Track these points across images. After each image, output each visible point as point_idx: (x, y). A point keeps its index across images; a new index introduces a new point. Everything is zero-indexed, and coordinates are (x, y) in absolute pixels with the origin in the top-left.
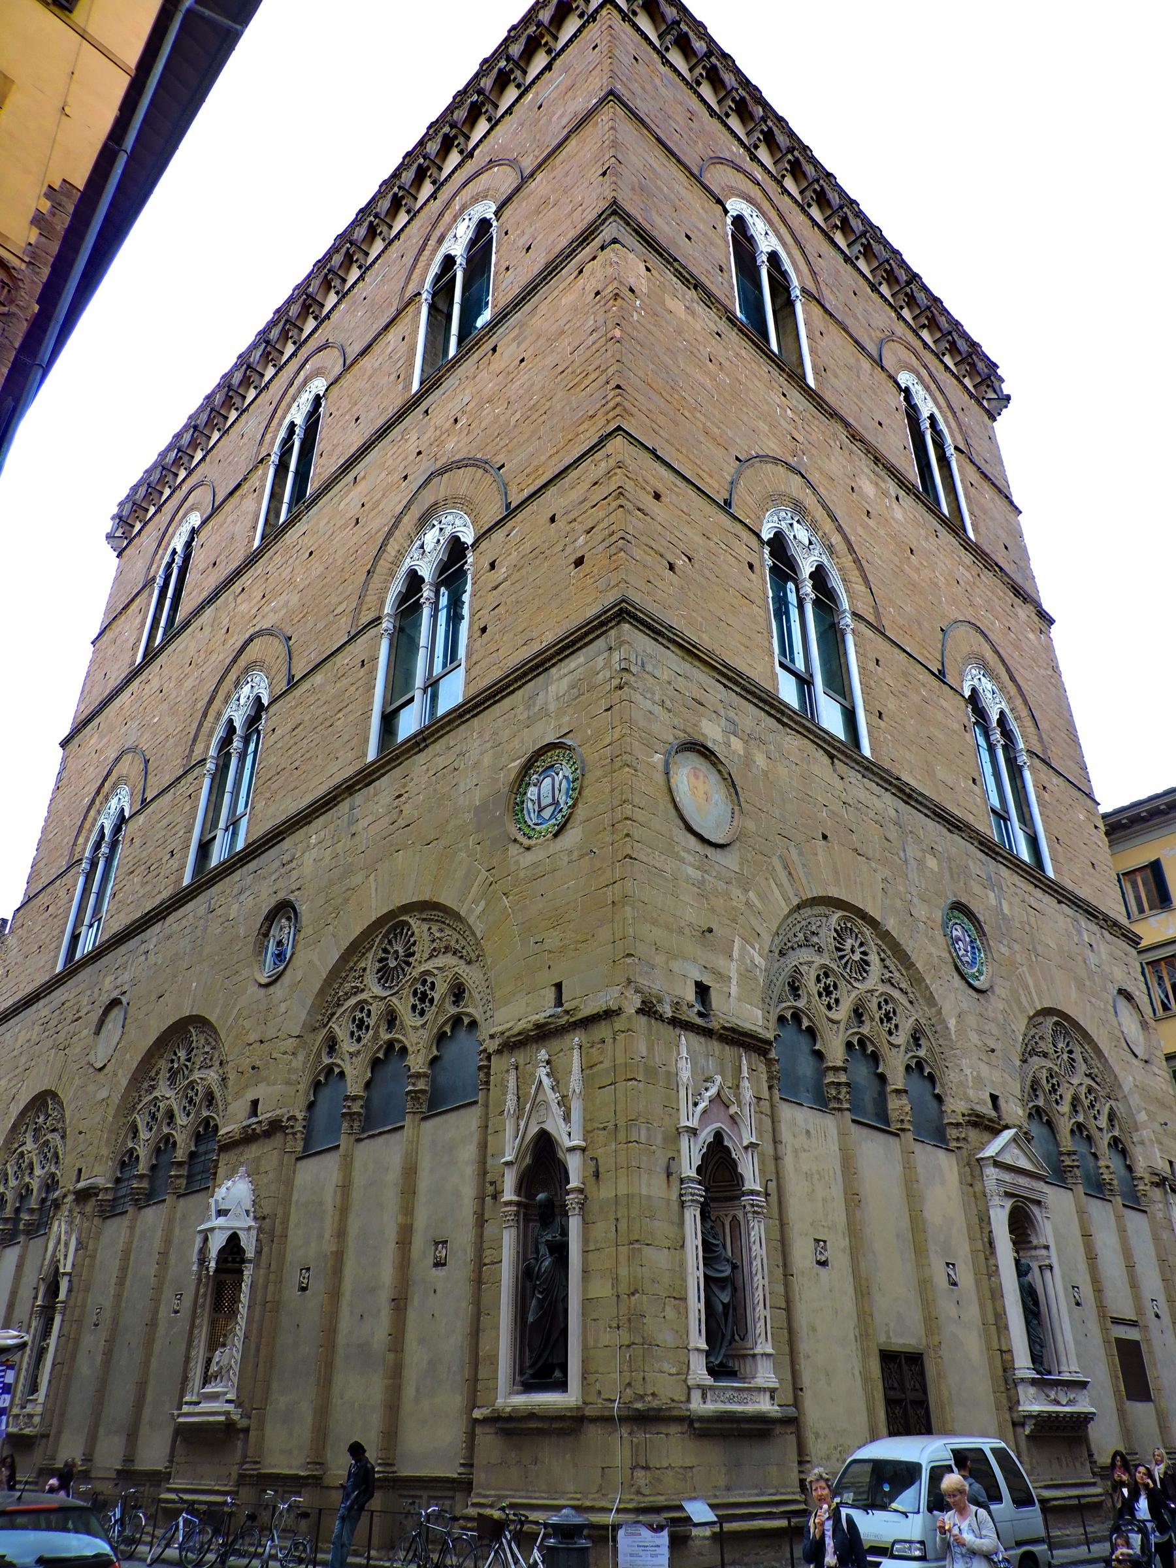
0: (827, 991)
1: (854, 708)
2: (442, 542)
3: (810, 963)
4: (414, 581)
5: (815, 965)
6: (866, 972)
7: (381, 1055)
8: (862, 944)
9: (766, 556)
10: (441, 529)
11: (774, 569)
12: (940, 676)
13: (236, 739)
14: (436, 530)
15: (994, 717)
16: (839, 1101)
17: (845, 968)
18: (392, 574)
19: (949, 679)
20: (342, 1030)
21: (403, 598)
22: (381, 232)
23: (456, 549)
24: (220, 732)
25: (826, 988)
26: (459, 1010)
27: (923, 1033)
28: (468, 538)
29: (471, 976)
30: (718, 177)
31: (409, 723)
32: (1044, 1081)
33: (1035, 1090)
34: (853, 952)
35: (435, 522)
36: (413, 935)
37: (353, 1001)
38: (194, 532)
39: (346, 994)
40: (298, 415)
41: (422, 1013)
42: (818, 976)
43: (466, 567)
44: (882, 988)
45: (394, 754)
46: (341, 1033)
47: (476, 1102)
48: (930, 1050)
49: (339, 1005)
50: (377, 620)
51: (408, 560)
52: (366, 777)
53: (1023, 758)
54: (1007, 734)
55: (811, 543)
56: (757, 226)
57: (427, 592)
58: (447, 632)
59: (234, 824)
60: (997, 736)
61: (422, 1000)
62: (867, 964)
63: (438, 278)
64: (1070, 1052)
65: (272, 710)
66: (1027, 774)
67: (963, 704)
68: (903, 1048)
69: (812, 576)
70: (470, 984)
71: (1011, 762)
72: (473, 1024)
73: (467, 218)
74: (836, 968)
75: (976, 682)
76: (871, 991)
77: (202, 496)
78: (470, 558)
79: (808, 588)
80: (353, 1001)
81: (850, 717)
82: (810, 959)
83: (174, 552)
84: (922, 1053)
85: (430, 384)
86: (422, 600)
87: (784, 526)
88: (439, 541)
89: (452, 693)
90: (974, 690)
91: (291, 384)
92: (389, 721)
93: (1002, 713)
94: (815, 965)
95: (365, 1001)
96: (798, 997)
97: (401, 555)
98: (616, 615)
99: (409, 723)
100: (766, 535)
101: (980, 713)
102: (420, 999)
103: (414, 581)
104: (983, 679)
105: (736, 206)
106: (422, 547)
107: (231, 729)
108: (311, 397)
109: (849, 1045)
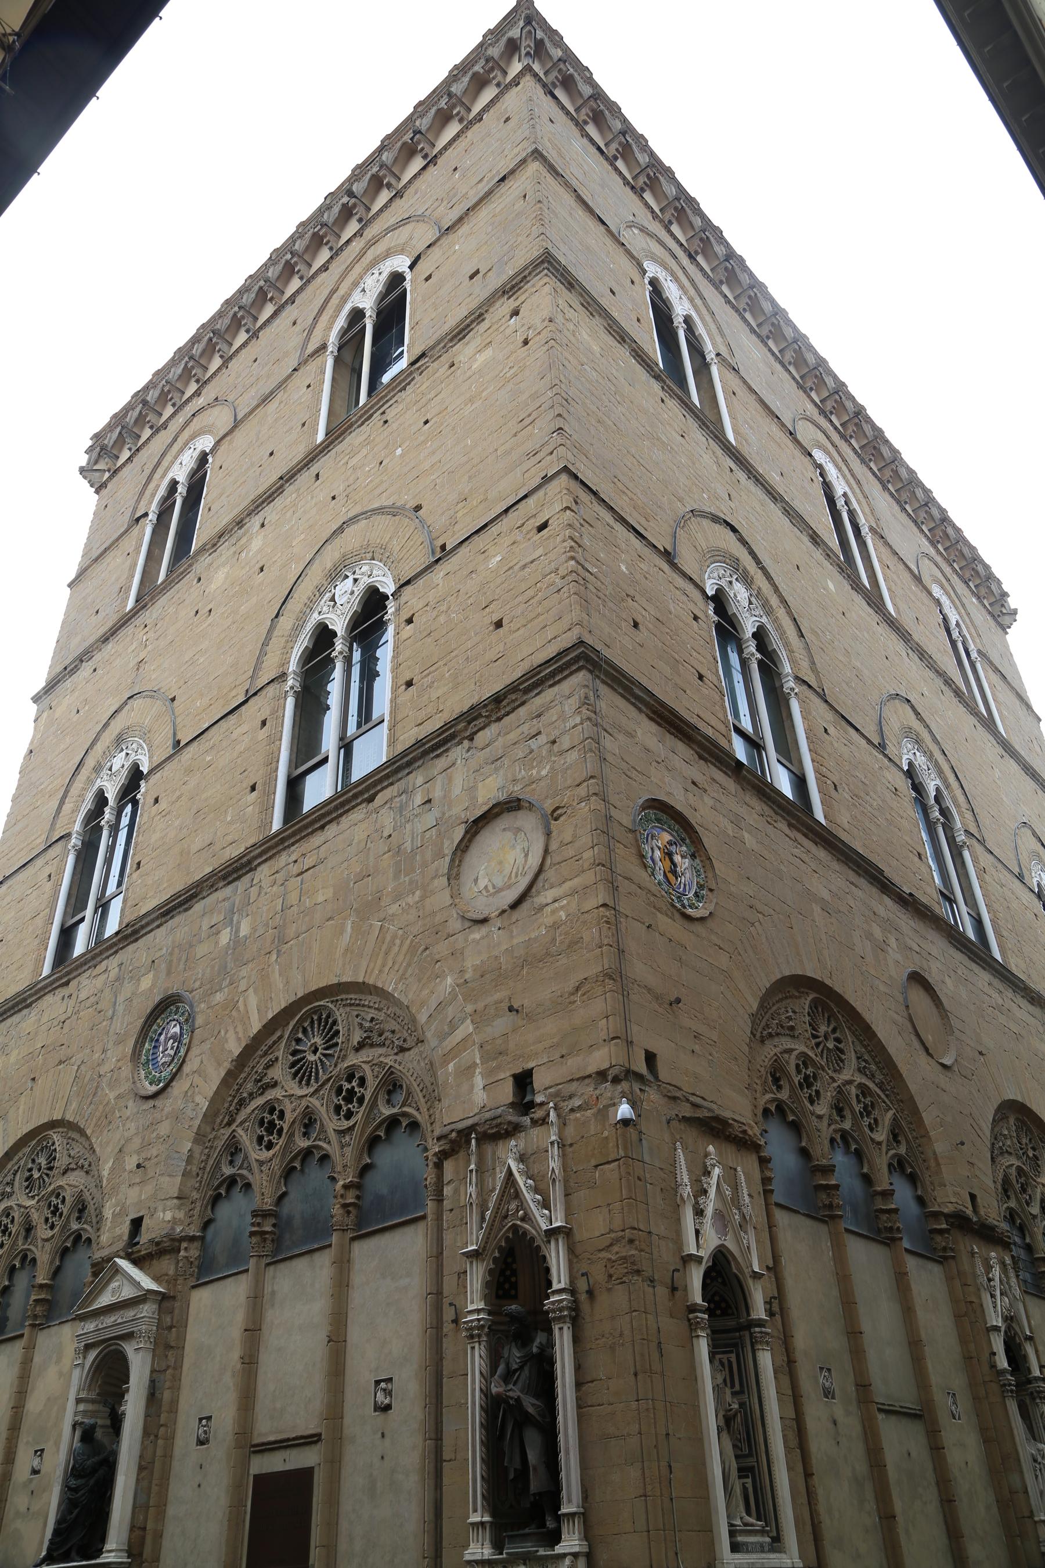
0: (808, 1082)
1: (804, 775)
3: (789, 1051)
4: (324, 636)
5: (795, 1053)
6: (842, 1061)
8: (834, 1031)
9: (711, 612)
10: (356, 580)
11: (719, 627)
12: (881, 747)
13: (107, 810)
14: (350, 580)
15: (933, 793)
16: (830, 1206)
17: (822, 1056)
18: (297, 629)
19: (891, 750)
21: (309, 655)
22: (299, 271)
24: (87, 805)
25: (806, 1078)
26: (395, 1110)
27: (900, 1127)
28: (388, 587)
29: (409, 1066)
30: (635, 240)
31: (319, 788)
32: (1014, 1182)
33: (1005, 1191)
34: (826, 1038)
35: (349, 574)
36: (335, 1023)
37: (260, 1101)
39: (251, 1094)
40: (181, 472)
41: (349, 1115)
42: (797, 1066)
43: (386, 617)
44: (860, 1079)
45: (300, 824)
46: (246, 1139)
47: (423, 1217)
48: (909, 1148)
49: (242, 1103)
51: (315, 615)
52: (271, 847)
53: (961, 837)
54: (944, 812)
55: (750, 603)
56: (672, 291)
57: (339, 645)
58: (361, 690)
59: (103, 906)
60: (936, 814)
61: (348, 1100)
62: (842, 1051)
63: (344, 332)
64: (1034, 1149)
65: (154, 779)
66: (966, 854)
67: (904, 777)
68: (884, 1146)
69: (755, 635)
70: (410, 1080)
71: (951, 840)
72: (414, 1126)
73: (376, 272)
74: (814, 1057)
75: (912, 757)
76: (850, 1082)
78: (391, 607)
79: (751, 647)
80: (260, 1101)
81: (800, 782)
82: (789, 1046)
84: (902, 1150)
85: (336, 433)
86: (333, 654)
87: (723, 583)
88: (352, 593)
89: (371, 754)
90: (911, 764)
91: (175, 440)
92: (295, 786)
93: (938, 790)
94: (795, 1053)
96: (779, 1088)
97: (310, 605)
98: (577, 659)
99: (319, 788)
100: (710, 592)
101: (918, 788)
102: (344, 1099)
103: (324, 636)
104: (918, 754)
105: (652, 269)
106: (333, 599)
107: (101, 800)
108: (196, 454)
109: (832, 1141)
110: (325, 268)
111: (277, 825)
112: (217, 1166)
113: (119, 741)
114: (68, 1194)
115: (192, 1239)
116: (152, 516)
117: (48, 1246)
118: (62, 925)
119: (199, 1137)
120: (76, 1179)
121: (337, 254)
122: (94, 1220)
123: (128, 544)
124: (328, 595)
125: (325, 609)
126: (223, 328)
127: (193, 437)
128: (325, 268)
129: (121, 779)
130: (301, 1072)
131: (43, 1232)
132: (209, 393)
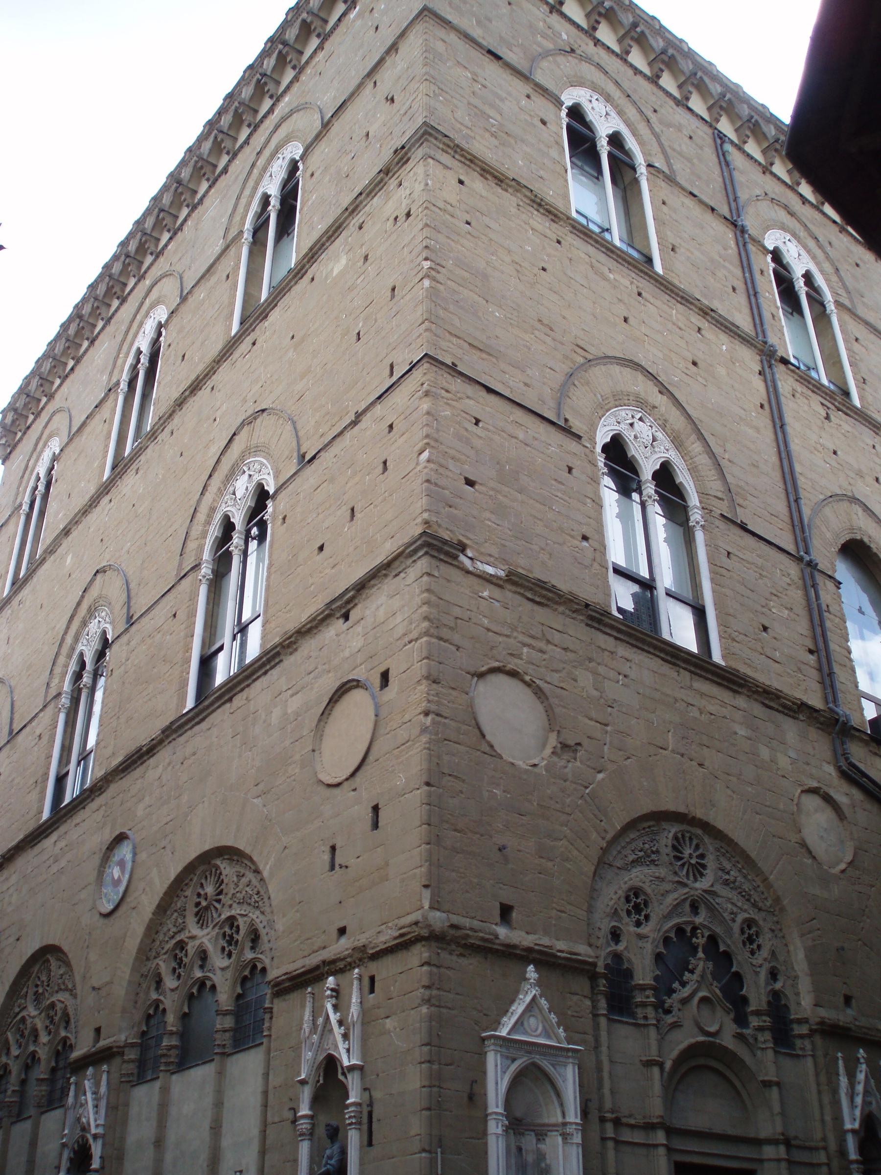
2: (250, 489)
4: (228, 527)
7: (195, 991)
10: (250, 476)
14: (246, 476)
20: (164, 967)
23: (262, 496)
24: (73, 667)
31: (224, 669)
35: (245, 468)
37: (174, 941)
38: (55, 458)
45: (210, 699)
50: (196, 567)
51: (223, 505)
77: (60, 422)
78: (270, 504)
83: (38, 479)
95: (181, 941)
99: (224, 669)
102: (227, 941)
106: (234, 494)
110: (247, 142)
111: (190, 703)
112: (147, 993)
113: (92, 612)
114: (59, 1006)
115: (132, 1045)
116: (124, 386)
117: (47, 1048)
118: (57, 776)
119: (134, 970)
120: (61, 996)
121: (214, 183)
122: (74, 1031)
123: (105, 412)
124: (231, 489)
125: (229, 503)
126: (118, 272)
127: (153, 306)
128: (247, 142)
129: (96, 645)
130: (202, 915)
131: (44, 1038)
132: (162, 265)
